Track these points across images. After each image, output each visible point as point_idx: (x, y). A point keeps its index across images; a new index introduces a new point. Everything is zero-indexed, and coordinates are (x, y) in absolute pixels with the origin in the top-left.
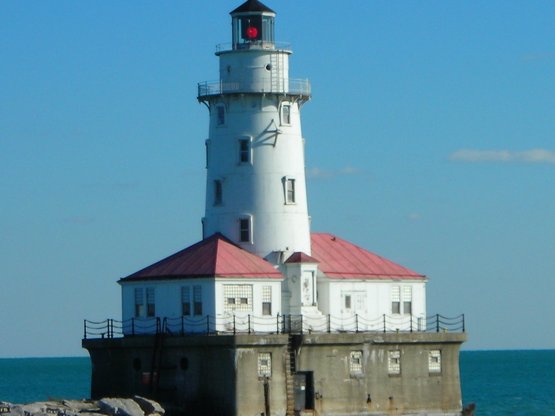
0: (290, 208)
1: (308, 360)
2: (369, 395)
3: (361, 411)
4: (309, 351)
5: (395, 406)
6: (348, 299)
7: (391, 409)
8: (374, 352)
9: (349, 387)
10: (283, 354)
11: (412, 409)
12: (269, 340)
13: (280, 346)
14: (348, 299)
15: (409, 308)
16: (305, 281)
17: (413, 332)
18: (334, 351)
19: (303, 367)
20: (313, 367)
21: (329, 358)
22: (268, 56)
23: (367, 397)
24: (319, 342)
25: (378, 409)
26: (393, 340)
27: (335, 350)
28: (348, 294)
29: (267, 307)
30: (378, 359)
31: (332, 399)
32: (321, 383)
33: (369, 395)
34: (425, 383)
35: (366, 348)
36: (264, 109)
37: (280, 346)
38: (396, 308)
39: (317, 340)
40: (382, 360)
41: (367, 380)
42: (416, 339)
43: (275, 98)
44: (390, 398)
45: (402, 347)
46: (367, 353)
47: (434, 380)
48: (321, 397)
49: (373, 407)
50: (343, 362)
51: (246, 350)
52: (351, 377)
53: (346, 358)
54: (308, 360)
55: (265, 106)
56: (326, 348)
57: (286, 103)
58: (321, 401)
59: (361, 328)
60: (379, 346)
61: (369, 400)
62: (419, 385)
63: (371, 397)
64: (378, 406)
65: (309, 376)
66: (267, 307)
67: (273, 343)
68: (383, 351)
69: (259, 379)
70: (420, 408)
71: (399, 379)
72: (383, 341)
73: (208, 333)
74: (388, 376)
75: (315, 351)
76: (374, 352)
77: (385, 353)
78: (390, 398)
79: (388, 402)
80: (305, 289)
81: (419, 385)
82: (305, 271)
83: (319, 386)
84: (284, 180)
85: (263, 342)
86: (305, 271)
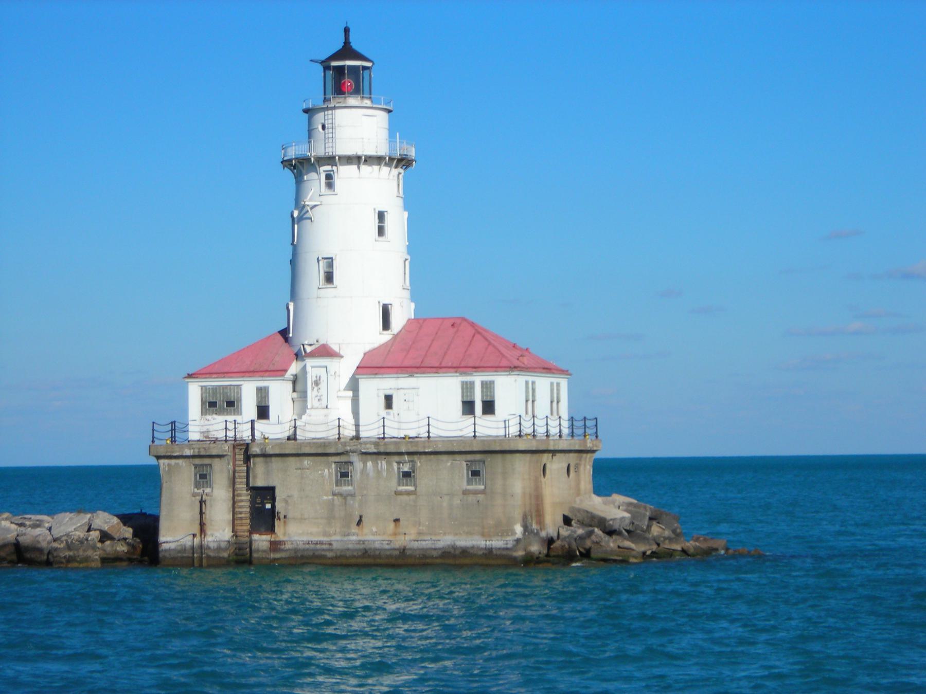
0: (329, 291)
1: (268, 473)
2: (361, 517)
4: (266, 462)
7: (395, 534)
8: (369, 464)
9: (331, 504)
11: (431, 534)
12: (196, 451)
13: (220, 456)
15: (489, 407)
16: (314, 379)
17: (342, 440)
18: (306, 462)
19: (260, 481)
21: (299, 471)
22: (322, 114)
23: (358, 519)
24: (271, 452)
25: (375, 534)
26: (392, 449)
27: (306, 462)
28: (389, 392)
29: (263, 412)
30: (379, 472)
31: (302, 520)
32: (286, 502)
33: (361, 517)
34: (457, 501)
35: (355, 458)
36: (305, 178)
37: (220, 456)
38: (468, 407)
39: (269, 450)
40: (385, 474)
41: (358, 498)
42: (429, 447)
43: (356, 161)
44: (397, 521)
45: (415, 458)
46: (358, 465)
47: (471, 498)
48: (285, 517)
49: (366, 530)
50: (322, 476)
51: (173, 462)
52: (334, 494)
53: (326, 471)
54: (268, 473)
55: (307, 173)
56: (292, 460)
57: (328, 168)
58: (285, 522)
59: (390, 432)
60: (374, 456)
61: (359, 523)
62: (445, 504)
63: (363, 519)
64: (374, 529)
65: (269, 492)
66: (263, 412)
67: (203, 453)
68: (384, 463)
69: (194, 495)
70: (445, 534)
71: (412, 497)
72: (375, 451)
73: (384, 438)
74: (393, 493)
75: (276, 463)
76: (369, 464)
77: (389, 464)
78: (397, 521)
79: (392, 525)
80: (316, 388)
81: (445, 504)
82: (313, 367)
83: (283, 504)
84: (318, 260)
85: (188, 452)
86: (313, 367)
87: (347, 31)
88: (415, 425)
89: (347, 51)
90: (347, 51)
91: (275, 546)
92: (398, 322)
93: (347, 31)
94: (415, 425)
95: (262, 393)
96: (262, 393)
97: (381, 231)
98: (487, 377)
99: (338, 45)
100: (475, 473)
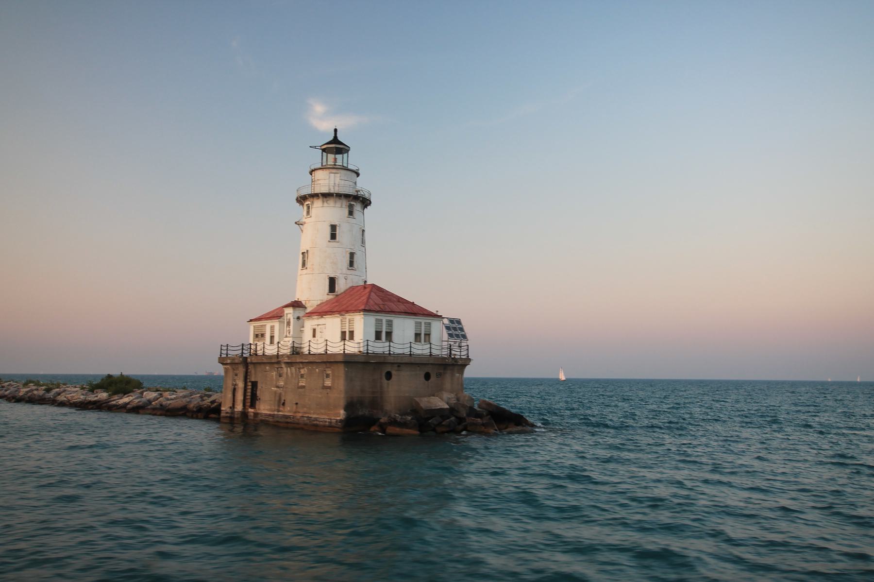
3: (279, 411)
5: (299, 410)
6: (314, 330)
9: (275, 392)
10: (241, 370)
14: (314, 330)
15: (352, 333)
19: (253, 380)
20: (259, 380)
25: (289, 411)
46: (285, 369)
56: (262, 366)
61: (284, 404)
65: (255, 384)
79: (295, 406)
87: (336, 130)
88: (401, 346)
89: (335, 140)
90: (335, 140)
91: (256, 414)
92: (341, 287)
93: (336, 130)
94: (401, 346)
95: (272, 328)
96: (272, 328)
97: (333, 236)
98: (389, 317)
99: (331, 138)
100: (328, 376)
